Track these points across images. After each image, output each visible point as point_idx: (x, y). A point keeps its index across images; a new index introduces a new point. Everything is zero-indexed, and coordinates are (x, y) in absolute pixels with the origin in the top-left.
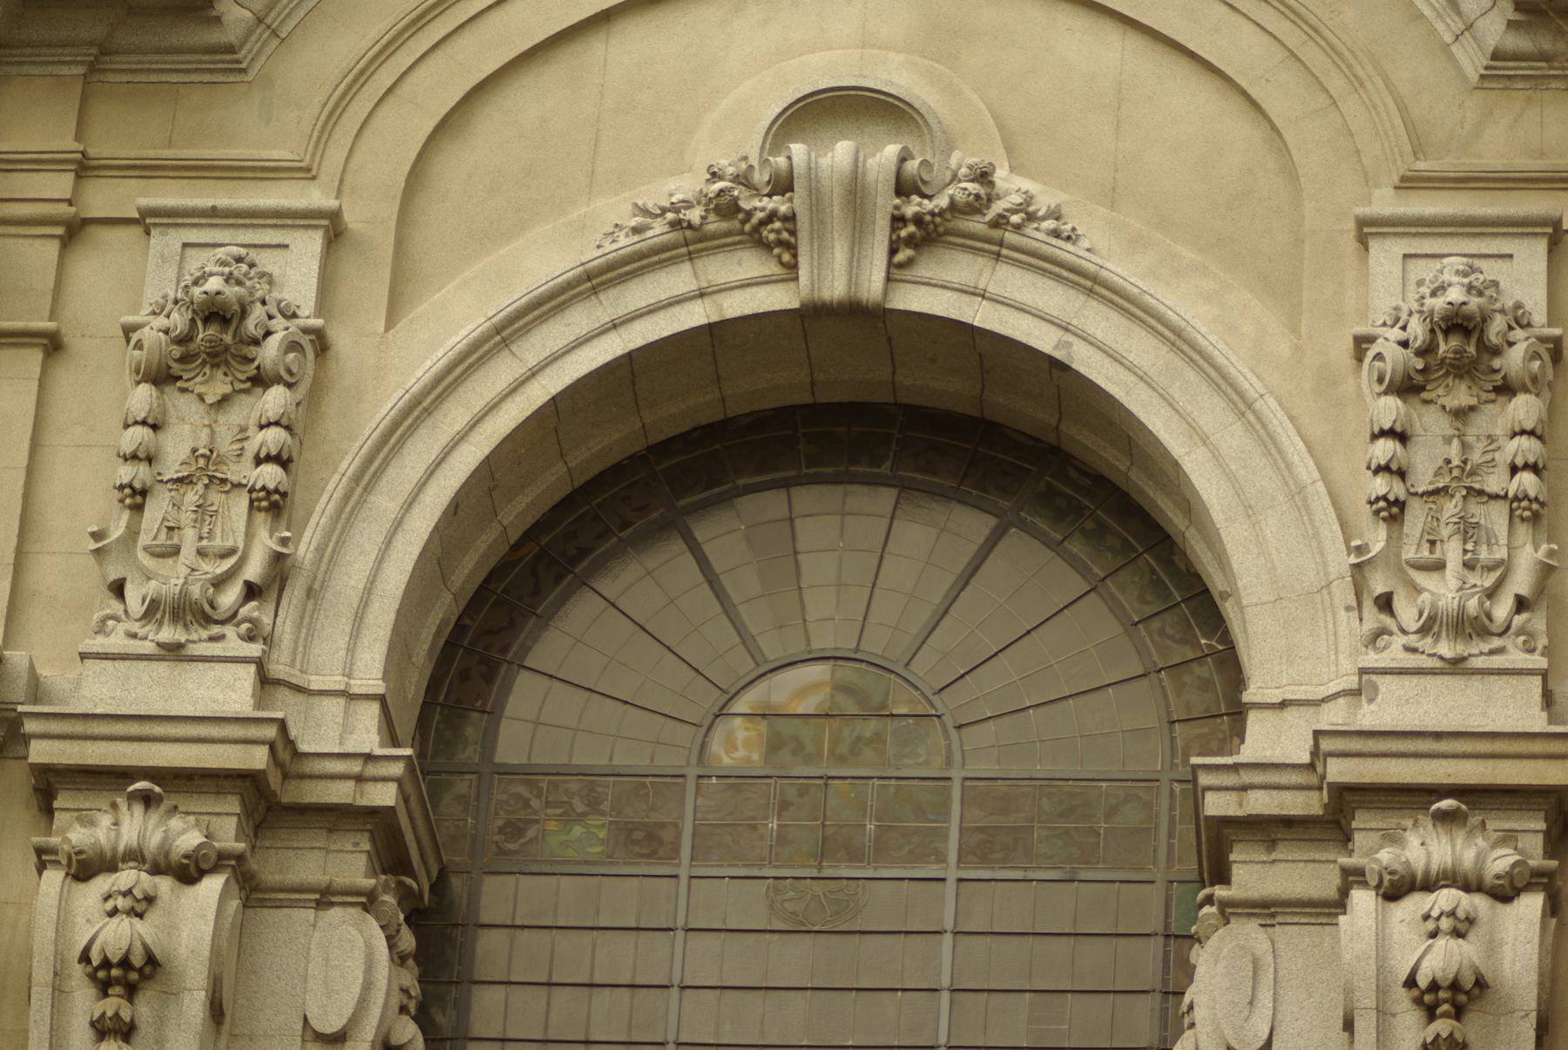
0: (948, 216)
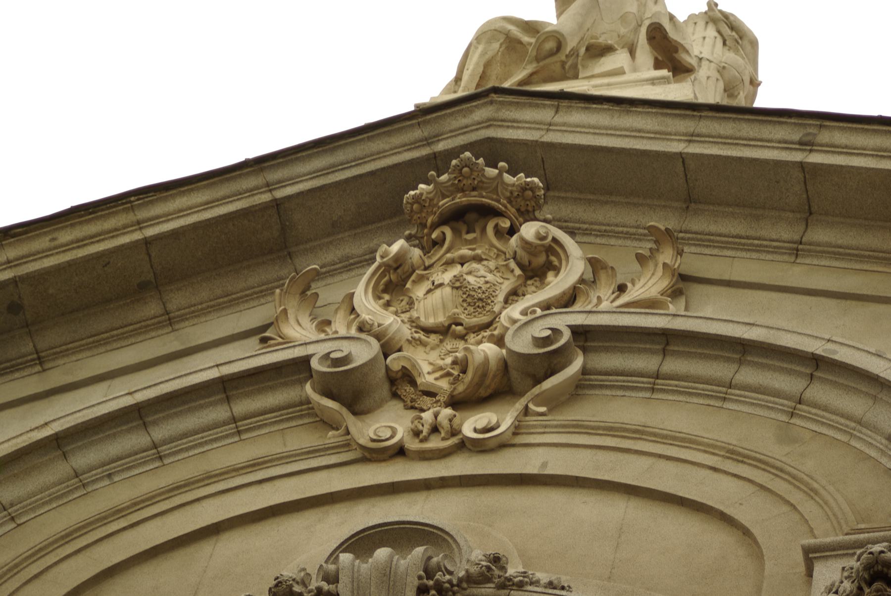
0: (465, 585)
